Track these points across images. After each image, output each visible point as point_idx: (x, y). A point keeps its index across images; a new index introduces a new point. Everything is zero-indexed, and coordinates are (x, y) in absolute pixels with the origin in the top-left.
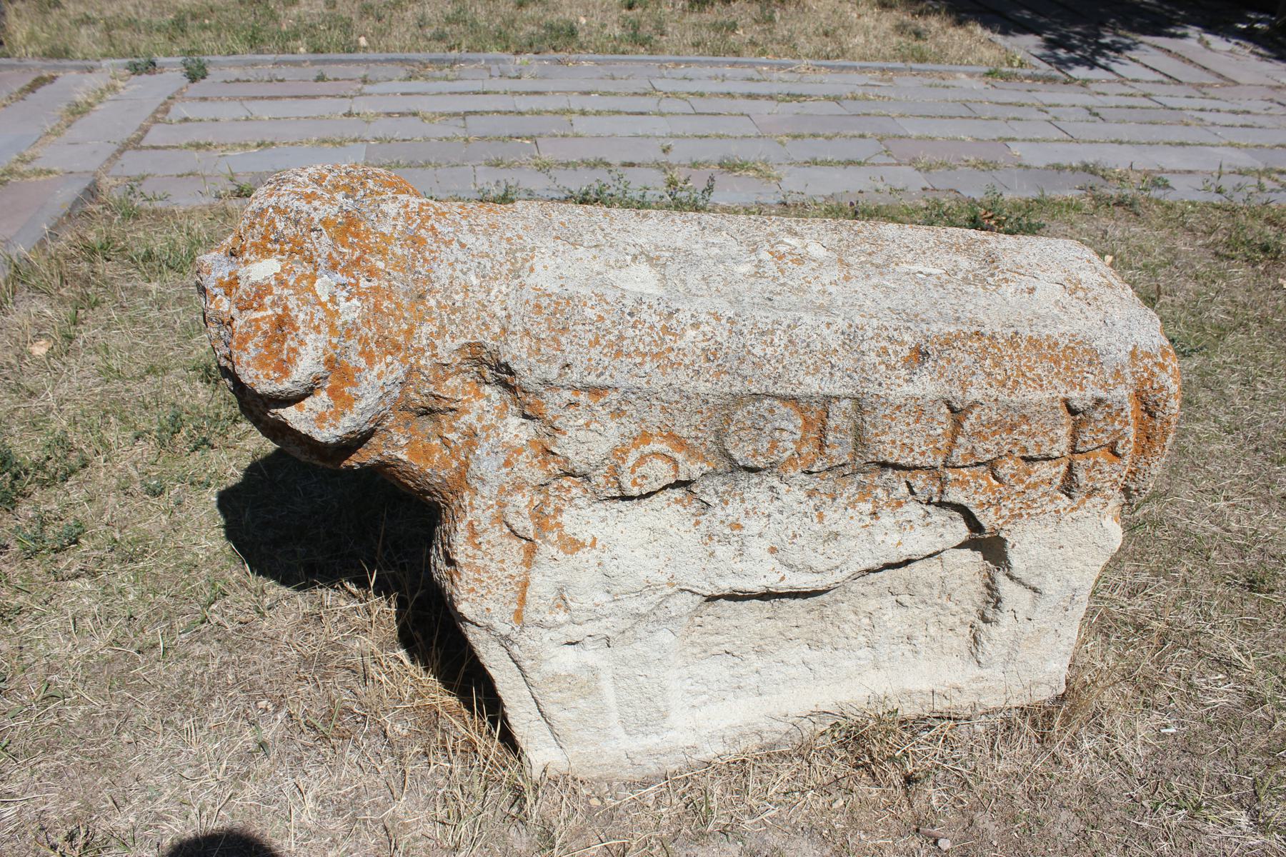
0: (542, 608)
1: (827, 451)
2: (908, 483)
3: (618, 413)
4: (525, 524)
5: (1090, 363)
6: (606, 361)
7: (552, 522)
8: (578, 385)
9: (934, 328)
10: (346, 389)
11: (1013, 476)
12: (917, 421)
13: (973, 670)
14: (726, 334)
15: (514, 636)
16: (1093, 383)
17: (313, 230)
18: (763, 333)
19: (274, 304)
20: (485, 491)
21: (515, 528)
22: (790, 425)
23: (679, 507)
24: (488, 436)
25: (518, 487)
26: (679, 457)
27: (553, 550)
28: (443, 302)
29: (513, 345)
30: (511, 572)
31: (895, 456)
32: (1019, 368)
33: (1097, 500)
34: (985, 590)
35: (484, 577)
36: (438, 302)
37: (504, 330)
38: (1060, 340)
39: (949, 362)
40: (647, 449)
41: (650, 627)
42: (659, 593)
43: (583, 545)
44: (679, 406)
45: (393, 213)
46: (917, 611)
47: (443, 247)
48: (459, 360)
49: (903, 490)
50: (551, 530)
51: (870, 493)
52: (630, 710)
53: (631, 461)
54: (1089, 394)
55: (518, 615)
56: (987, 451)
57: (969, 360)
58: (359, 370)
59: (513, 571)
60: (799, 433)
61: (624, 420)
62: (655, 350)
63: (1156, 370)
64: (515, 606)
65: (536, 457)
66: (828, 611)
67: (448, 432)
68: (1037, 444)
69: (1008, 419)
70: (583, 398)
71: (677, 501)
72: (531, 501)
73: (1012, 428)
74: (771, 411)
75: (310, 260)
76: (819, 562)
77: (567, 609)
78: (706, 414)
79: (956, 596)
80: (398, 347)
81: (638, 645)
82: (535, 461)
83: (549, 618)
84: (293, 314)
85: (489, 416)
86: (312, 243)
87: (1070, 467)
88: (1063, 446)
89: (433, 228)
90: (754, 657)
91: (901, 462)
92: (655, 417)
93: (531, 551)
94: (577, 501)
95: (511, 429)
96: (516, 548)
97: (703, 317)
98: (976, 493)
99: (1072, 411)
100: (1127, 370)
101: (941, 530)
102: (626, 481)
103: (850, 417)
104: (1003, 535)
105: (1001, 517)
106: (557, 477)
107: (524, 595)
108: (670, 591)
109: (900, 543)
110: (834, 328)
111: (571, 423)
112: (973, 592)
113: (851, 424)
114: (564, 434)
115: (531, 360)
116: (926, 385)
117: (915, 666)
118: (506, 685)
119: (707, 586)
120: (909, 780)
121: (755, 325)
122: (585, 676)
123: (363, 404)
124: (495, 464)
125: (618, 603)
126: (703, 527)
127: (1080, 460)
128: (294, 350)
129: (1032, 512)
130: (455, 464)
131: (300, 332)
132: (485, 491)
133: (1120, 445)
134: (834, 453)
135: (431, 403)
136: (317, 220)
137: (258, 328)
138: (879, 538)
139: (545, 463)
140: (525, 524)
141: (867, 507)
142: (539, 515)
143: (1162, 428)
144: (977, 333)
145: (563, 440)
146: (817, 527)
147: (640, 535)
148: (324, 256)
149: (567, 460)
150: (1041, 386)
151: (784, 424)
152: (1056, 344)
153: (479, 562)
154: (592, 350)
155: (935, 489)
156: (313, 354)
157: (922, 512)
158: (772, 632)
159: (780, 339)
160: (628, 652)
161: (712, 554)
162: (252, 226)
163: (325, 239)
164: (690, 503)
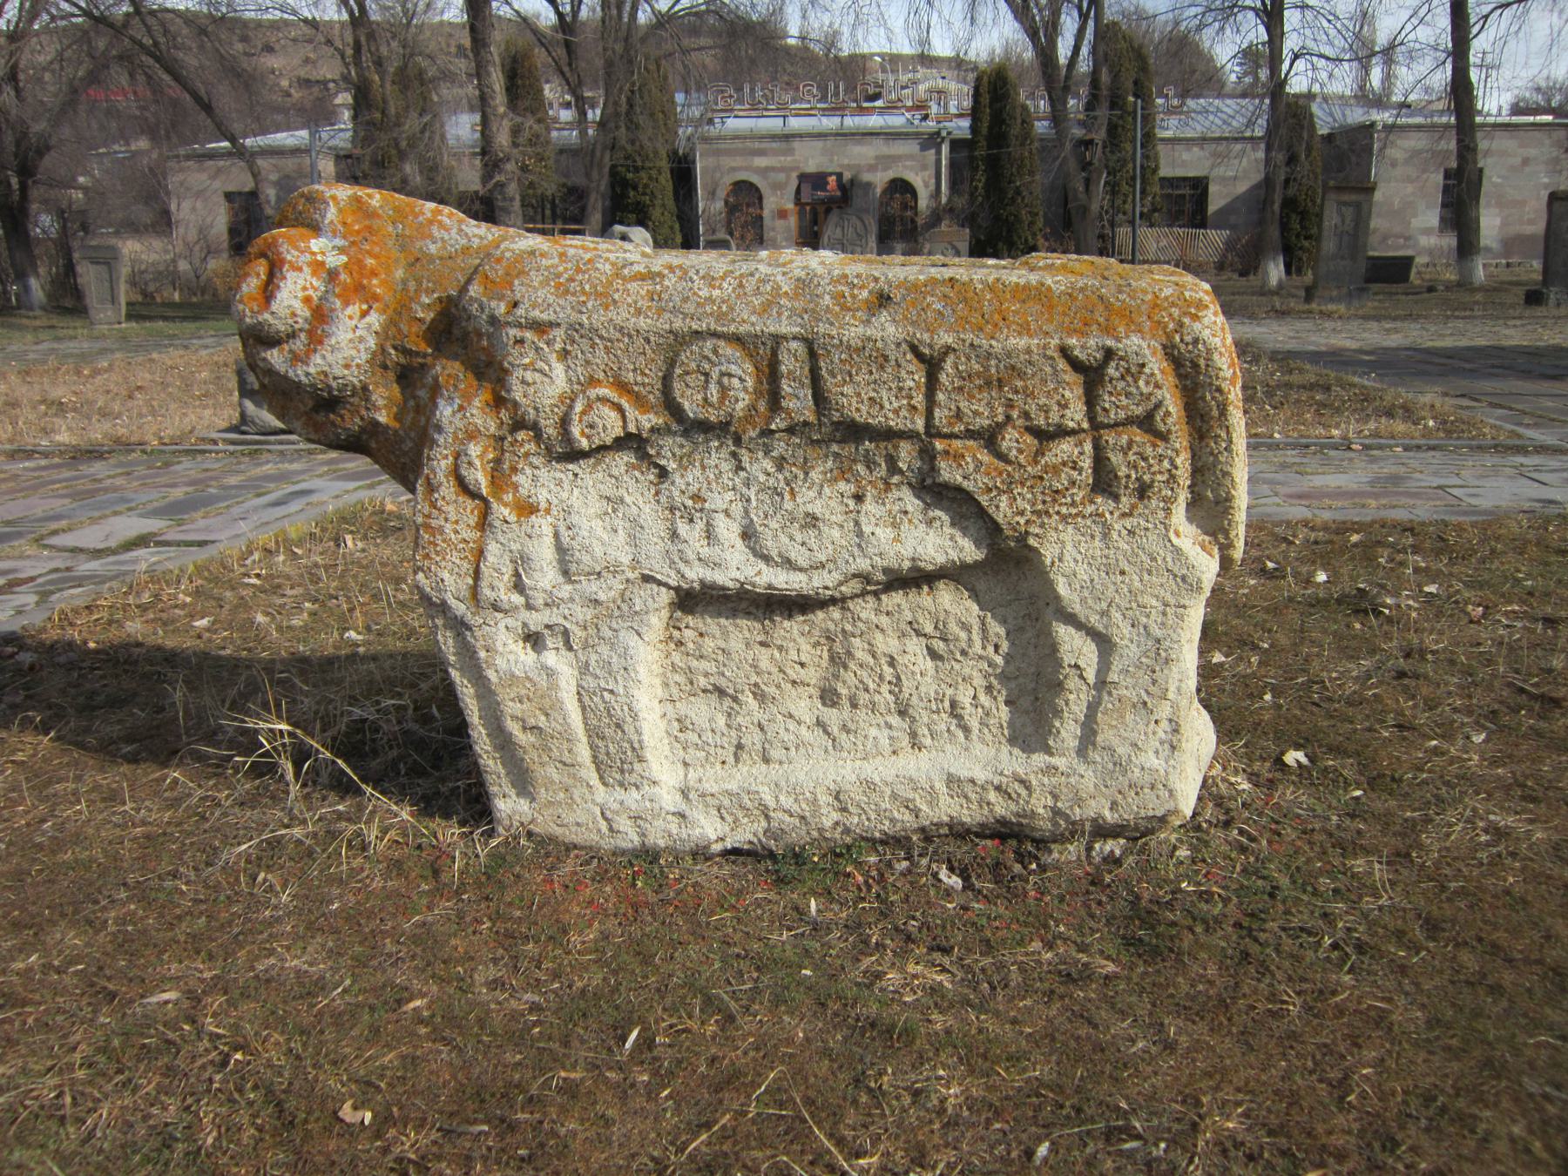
3: (564, 354)
4: (479, 477)
27: (506, 512)
40: (593, 393)
53: (578, 408)
54: (1092, 342)
55: (475, 591)
56: (976, 413)
63: (1186, 320)
68: (1041, 408)
70: (528, 335)
74: (715, 352)
76: (799, 555)
87: (1098, 448)
88: (1076, 414)
102: (576, 431)
104: (1032, 541)
105: (1022, 513)
107: (478, 566)
116: (887, 329)
127: (1109, 437)
129: (1064, 510)
141: (847, 488)
151: (733, 369)
153: (434, 523)
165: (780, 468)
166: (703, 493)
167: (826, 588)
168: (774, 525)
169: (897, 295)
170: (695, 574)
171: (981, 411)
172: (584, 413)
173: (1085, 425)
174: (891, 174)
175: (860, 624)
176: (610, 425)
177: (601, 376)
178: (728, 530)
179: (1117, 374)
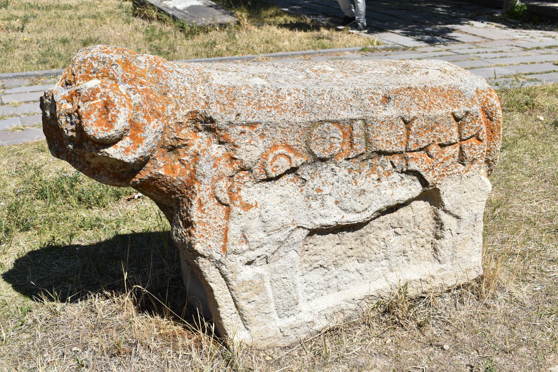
0: (236, 242)
1: (355, 147)
2: (391, 162)
3: (262, 136)
4: (224, 196)
5: (460, 96)
6: (255, 111)
7: (236, 195)
8: (244, 123)
9: (391, 87)
10: (139, 135)
11: (437, 154)
12: (391, 128)
13: (437, 266)
14: (303, 96)
15: (223, 260)
16: (463, 105)
17: (113, 65)
18: (319, 95)
19: (102, 96)
20: (205, 181)
21: (220, 199)
22: (337, 133)
24: (204, 154)
25: (220, 178)
26: (291, 155)
27: (239, 209)
28: (176, 95)
29: (213, 108)
30: (220, 224)
32: (430, 100)
33: (476, 165)
34: (434, 222)
35: (207, 227)
36: (174, 95)
37: (206, 103)
38: (445, 88)
39: (400, 101)
41: (286, 250)
42: (288, 229)
43: (252, 206)
44: (289, 130)
45: (144, 61)
46: (405, 237)
47: (170, 73)
48: (187, 120)
49: (390, 166)
50: (236, 200)
51: (375, 169)
52: (280, 301)
53: (270, 159)
54: (462, 109)
55: (224, 248)
56: (423, 141)
57: (408, 99)
58: (144, 125)
59: (221, 223)
61: (265, 139)
62: (275, 105)
63: (488, 97)
64: (222, 243)
65: (227, 162)
66: (364, 239)
67: (184, 156)
69: (430, 125)
70: (247, 129)
71: (291, 180)
72: (227, 184)
73: (432, 129)
74: (329, 129)
75: (113, 79)
76: (359, 207)
77: (247, 242)
78: (301, 133)
79: (422, 226)
80: (159, 115)
81: (281, 260)
82: (227, 164)
83: (239, 248)
84: (112, 99)
85: (203, 145)
86: (114, 71)
87: (461, 148)
88: (455, 138)
89: (163, 66)
90: (333, 268)
91: (387, 150)
92: (279, 136)
93: (228, 212)
94: (247, 184)
95: (214, 150)
96: (221, 210)
97: (292, 91)
98: (422, 164)
99: (457, 119)
100: (476, 98)
101: (409, 187)
102: (269, 169)
103: (362, 129)
104: (438, 186)
106: (238, 171)
107: (226, 236)
109: (392, 194)
110: (348, 91)
111: (243, 142)
112: (428, 224)
113: (363, 133)
114: (240, 148)
115: (222, 113)
116: (392, 111)
117: (409, 268)
118: (219, 292)
119: (309, 224)
120: (420, 326)
121: (315, 92)
122: (258, 281)
123: (147, 141)
124: (209, 166)
125: (270, 237)
126: (304, 192)
127: (464, 144)
128: (115, 116)
129: (449, 173)
130: (188, 172)
131: (117, 107)
132: (205, 181)
133: (480, 135)
134: (358, 147)
135: (175, 143)
136: (114, 61)
137: (96, 107)
138: (383, 192)
139: (232, 164)
142: (230, 192)
143: (497, 125)
145: (239, 150)
146: (355, 188)
147: (276, 199)
148: (120, 76)
149: (242, 161)
152: (443, 89)
153: (204, 220)
154: (248, 107)
155: (404, 164)
156: (124, 117)
157: (399, 177)
158: (340, 252)
159: (327, 97)
160: (277, 265)
161: (310, 207)
162: (80, 68)
163: (120, 68)
164: (297, 181)
166: (321, 188)
167: (368, 218)
170: (319, 222)
175: (373, 228)
176: (284, 164)
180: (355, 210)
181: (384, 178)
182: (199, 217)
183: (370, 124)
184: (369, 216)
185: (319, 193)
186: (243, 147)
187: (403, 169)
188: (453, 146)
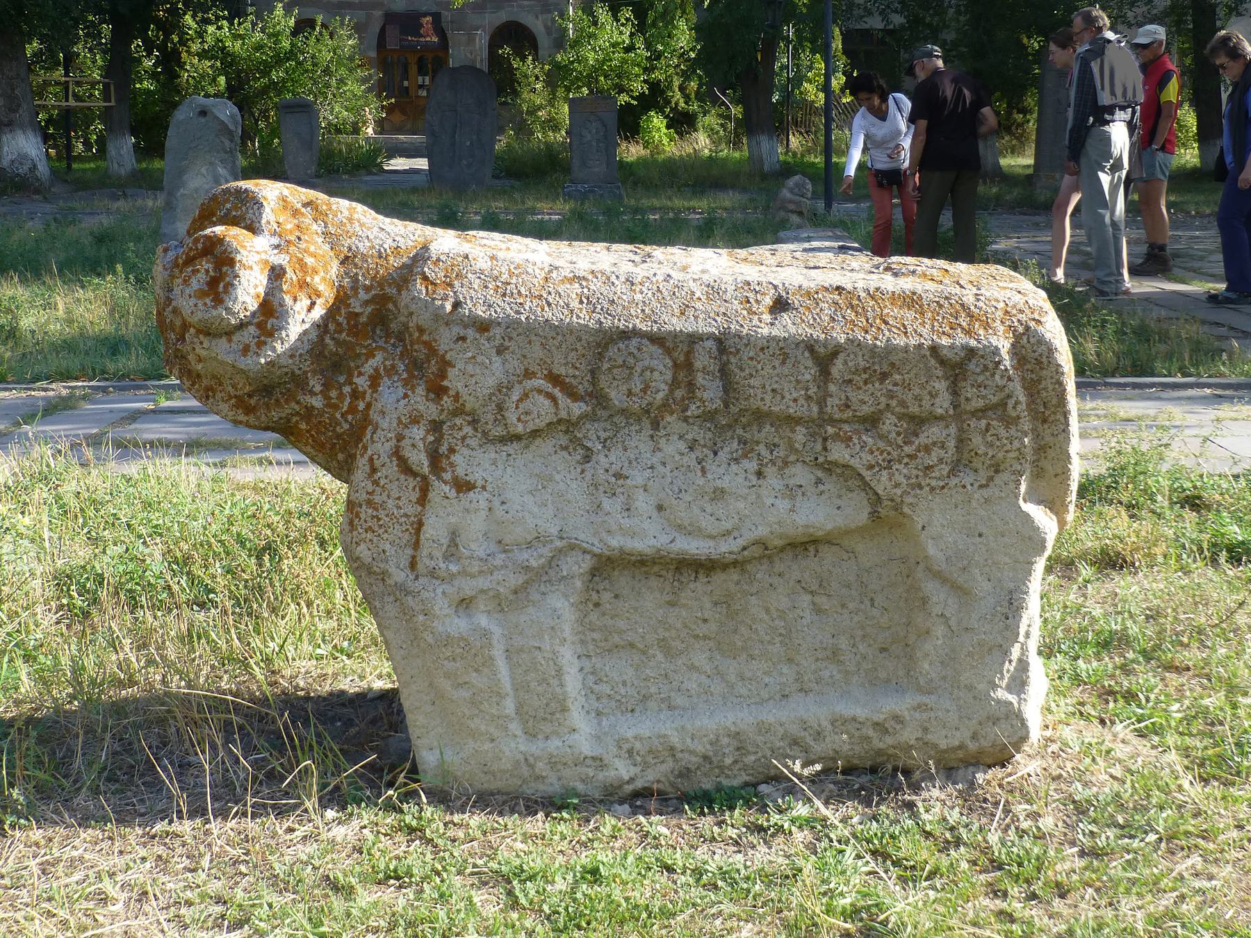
1: (698, 393)
4: (419, 459)
12: (783, 363)
23: (565, 453)
25: (415, 421)
31: (769, 403)
35: (382, 514)
40: (529, 384)
41: (543, 588)
50: (445, 471)
55: (413, 565)
59: (410, 510)
60: (669, 376)
63: (1032, 324)
70: (470, 333)
73: (884, 376)
76: (707, 523)
88: (943, 404)
94: (468, 441)
102: (512, 417)
104: (906, 510)
105: (897, 485)
108: (559, 544)
126: (588, 475)
129: (934, 483)
132: (384, 424)
133: (1010, 406)
134: (705, 396)
140: (419, 459)
141: (752, 465)
144: (838, 288)
145: (452, 373)
146: (701, 482)
150: (906, 333)
155: (819, 447)
157: (812, 477)
164: (575, 449)
165: (691, 449)
166: (624, 472)
168: (688, 498)
169: (795, 300)
171: (866, 400)
172: (520, 400)
173: (951, 412)
174: (502, 17)
176: (542, 411)
177: (536, 368)
178: (643, 503)
179: (978, 370)
180: (700, 530)
181: (770, 471)
182: (368, 493)
183: (733, 350)
184: (736, 550)
185: (620, 482)
186: (460, 365)
187: (816, 459)
188: (943, 424)
